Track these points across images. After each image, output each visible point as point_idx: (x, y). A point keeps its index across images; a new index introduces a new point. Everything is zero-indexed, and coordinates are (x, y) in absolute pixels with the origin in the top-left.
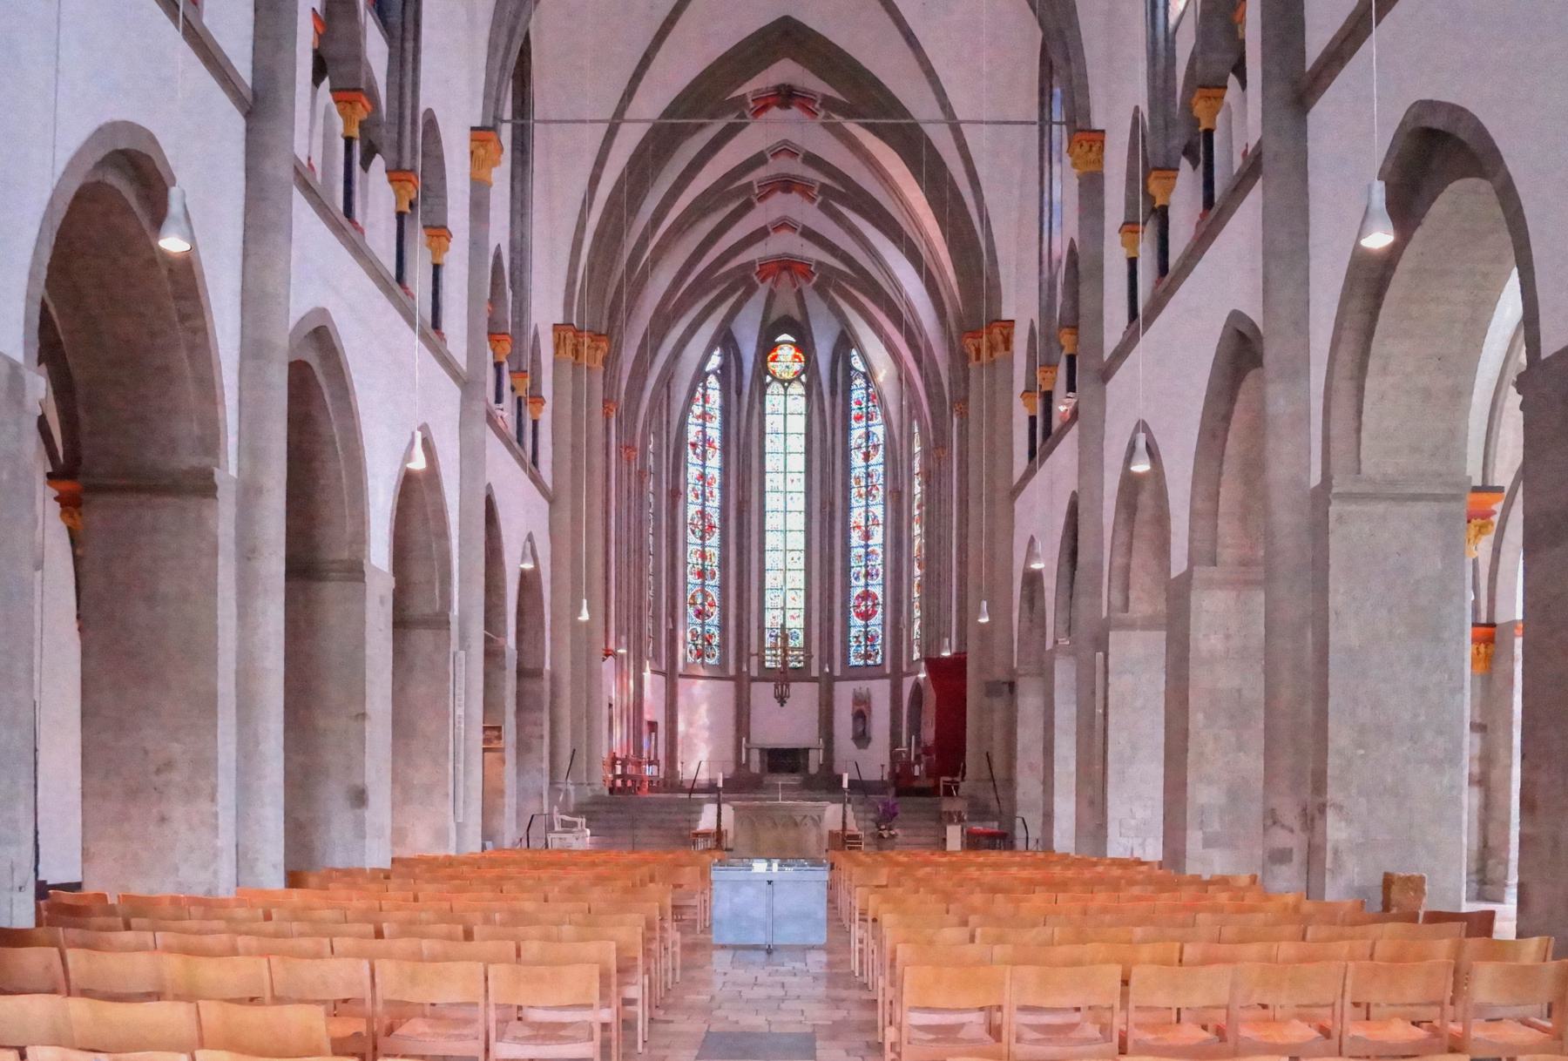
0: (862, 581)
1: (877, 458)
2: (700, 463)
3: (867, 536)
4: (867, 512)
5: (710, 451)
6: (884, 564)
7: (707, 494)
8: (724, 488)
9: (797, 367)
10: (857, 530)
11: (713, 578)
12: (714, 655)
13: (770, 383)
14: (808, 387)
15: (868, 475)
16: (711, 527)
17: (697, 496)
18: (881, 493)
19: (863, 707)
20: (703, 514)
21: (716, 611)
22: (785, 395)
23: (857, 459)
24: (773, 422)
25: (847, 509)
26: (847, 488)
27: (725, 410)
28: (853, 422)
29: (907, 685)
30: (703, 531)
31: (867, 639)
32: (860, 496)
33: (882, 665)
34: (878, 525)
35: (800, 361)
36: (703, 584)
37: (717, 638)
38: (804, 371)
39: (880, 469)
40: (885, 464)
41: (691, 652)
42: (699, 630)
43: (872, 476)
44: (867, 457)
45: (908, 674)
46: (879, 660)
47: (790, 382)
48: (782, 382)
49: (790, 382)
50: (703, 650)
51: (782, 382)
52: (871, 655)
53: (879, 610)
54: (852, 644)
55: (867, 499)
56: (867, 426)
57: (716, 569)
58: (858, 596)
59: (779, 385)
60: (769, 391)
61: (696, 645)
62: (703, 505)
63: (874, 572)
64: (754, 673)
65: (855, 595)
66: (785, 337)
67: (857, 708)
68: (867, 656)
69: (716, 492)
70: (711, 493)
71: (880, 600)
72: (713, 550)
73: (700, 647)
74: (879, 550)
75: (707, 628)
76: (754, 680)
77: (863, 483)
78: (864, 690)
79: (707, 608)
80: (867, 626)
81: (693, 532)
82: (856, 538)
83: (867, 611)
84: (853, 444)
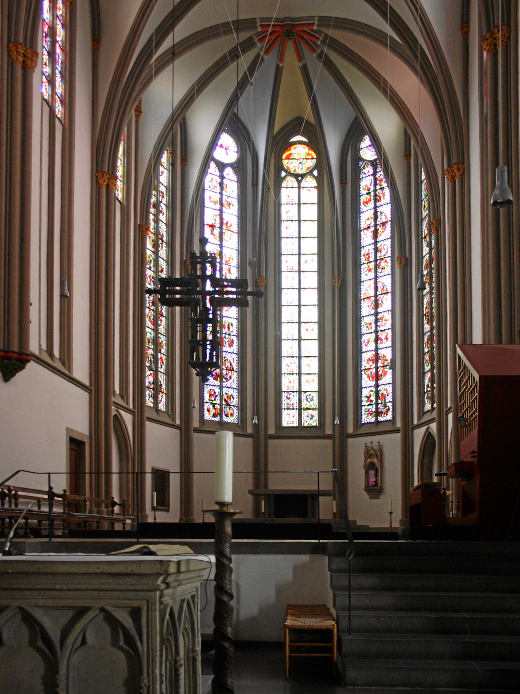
0: (372, 346)
1: (386, 234)
2: (219, 243)
4: (376, 283)
9: (311, 163)
10: (366, 301)
11: (231, 345)
12: (232, 415)
13: (285, 177)
14: (319, 179)
15: (376, 250)
18: (389, 264)
19: (375, 460)
22: (299, 188)
23: (366, 238)
25: (357, 282)
26: (357, 265)
28: (362, 206)
29: (419, 435)
33: (393, 421)
34: (387, 293)
35: (313, 158)
37: (236, 399)
38: (316, 167)
39: (388, 243)
40: (392, 238)
41: (208, 410)
42: (217, 391)
43: (381, 251)
44: (376, 234)
45: (419, 426)
46: (389, 417)
47: (303, 176)
48: (296, 176)
49: (303, 176)
50: (221, 409)
51: (296, 176)
52: (381, 412)
55: (376, 271)
56: (375, 207)
57: (235, 339)
58: (369, 360)
59: (294, 179)
60: (284, 184)
61: (214, 405)
64: (271, 431)
65: (366, 360)
66: (299, 138)
67: (369, 460)
68: (378, 413)
70: (229, 271)
73: (218, 406)
74: (388, 316)
75: (224, 390)
76: (272, 437)
77: (372, 259)
78: (375, 446)
80: (377, 386)
82: (366, 308)
83: (377, 372)
84: (363, 225)
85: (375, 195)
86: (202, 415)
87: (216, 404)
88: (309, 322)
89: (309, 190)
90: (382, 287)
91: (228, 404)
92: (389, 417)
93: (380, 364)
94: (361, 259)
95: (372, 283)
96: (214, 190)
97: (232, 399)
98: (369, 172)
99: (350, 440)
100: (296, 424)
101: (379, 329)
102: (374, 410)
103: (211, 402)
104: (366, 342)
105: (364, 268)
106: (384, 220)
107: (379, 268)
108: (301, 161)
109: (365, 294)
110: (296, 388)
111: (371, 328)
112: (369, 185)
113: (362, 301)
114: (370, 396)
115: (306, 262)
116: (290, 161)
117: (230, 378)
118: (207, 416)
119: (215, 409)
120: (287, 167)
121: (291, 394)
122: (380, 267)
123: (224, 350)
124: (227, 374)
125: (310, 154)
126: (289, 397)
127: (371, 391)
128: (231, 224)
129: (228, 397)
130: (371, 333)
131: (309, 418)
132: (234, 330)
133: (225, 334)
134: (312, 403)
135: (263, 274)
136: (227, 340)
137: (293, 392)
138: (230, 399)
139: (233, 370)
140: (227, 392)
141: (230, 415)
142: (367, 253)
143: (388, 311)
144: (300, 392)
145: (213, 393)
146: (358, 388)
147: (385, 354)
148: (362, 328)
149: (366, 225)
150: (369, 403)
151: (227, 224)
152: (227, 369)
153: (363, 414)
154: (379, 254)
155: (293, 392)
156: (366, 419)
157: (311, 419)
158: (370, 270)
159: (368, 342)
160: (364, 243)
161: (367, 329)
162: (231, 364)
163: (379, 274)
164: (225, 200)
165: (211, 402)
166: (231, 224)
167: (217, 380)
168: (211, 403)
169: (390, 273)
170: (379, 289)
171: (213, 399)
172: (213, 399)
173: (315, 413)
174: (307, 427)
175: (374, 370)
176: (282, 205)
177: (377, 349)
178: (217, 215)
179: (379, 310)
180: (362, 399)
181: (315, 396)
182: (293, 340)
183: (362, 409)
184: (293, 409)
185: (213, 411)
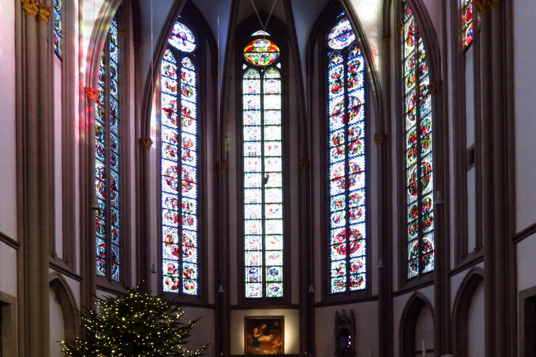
0: (343, 222)
2: (176, 127)
3: (347, 183)
5: (185, 121)
6: (367, 204)
8: (201, 151)
12: (192, 287)
15: (347, 133)
16: (189, 182)
17: (172, 154)
18: (363, 145)
19: (347, 326)
22: (262, 79)
26: (325, 149)
27: (201, 86)
30: (179, 183)
32: (339, 152)
34: (360, 172)
35: (276, 52)
37: (196, 273)
46: (363, 286)
47: (267, 68)
49: (267, 68)
54: (333, 275)
57: (194, 218)
58: (339, 235)
59: (255, 71)
60: (245, 76)
61: (173, 279)
63: (356, 212)
65: (335, 235)
67: (340, 327)
69: (193, 154)
72: (190, 201)
73: (177, 280)
75: (184, 265)
77: (342, 142)
78: (348, 314)
80: (348, 259)
82: (335, 188)
85: (346, 81)
86: (161, 286)
87: (175, 277)
88: (274, 203)
89: (273, 82)
90: (354, 167)
91: (188, 278)
92: (363, 286)
93: (352, 239)
94: (329, 143)
95: (342, 165)
96: (172, 77)
97: (192, 273)
98: (338, 60)
99: (318, 310)
100: (260, 296)
101: (350, 206)
102: (345, 281)
103: (170, 275)
105: (333, 151)
106: (356, 103)
107: (351, 150)
108: (264, 54)
109: (335, 175)
110: (260, 263)
111: (341, 206)
112: (338, 73)
113: (331, 182)
114: (340, 269)
115: (270, 148)
116: (251, 54)
118: (166, 288)
119: (175, 282)
120: (248, 59)
121: (254, 269)
122: (352, 148)
123: (183, 228)
124: (186, 250)
125: (274, 48)
126: (252, 271)
127: (342, 264)
128: (189, 110)
129: (187, 271)
130: (342, 210)
131: (273, 290)
132: (194, 209)
133: (185, 213)
134: (276, 277)
136: (186, 218)
137: (257, 267)
138: (190, 273)
139: (193, 246)
140: (186, 267)
141: (190, 288)
142: (336, 136)
143: (362, 189)
144: (264, 267)
145: (172, 267)
146: (327, 262)
147: (357, 229)
148: (331, 206)
149: (335, 111)
150: (339, 275)
151: (185, 109)
152: (186, 245)
153: (332, 285)
154: (350, 137)
155: (257, 267)
156: (335, 290)
157: (276, 291)
158: (339, 152)
159: (338, 220)
160: (332, 128)
161: (337, 207)
162: (191, 241)
163: (350, 155)
164: (183, 87)
165: (170, 275)
166: (189, 110)
167: (176, 255)
168: (170, 277)
169: (363, 153)
170: (351, 169)
171: (172, 272)
172: (172, 272)
173: (280, 286)
174: (271, 298)
175: (345, 245)
176: (244, 96)
178: (174, 101)
179: (351, 188)
180: (332, 271)
181: (280, 270)
182: (256, 219)
183: (331, 281)
184: (257, 282)
185: (172, 284)
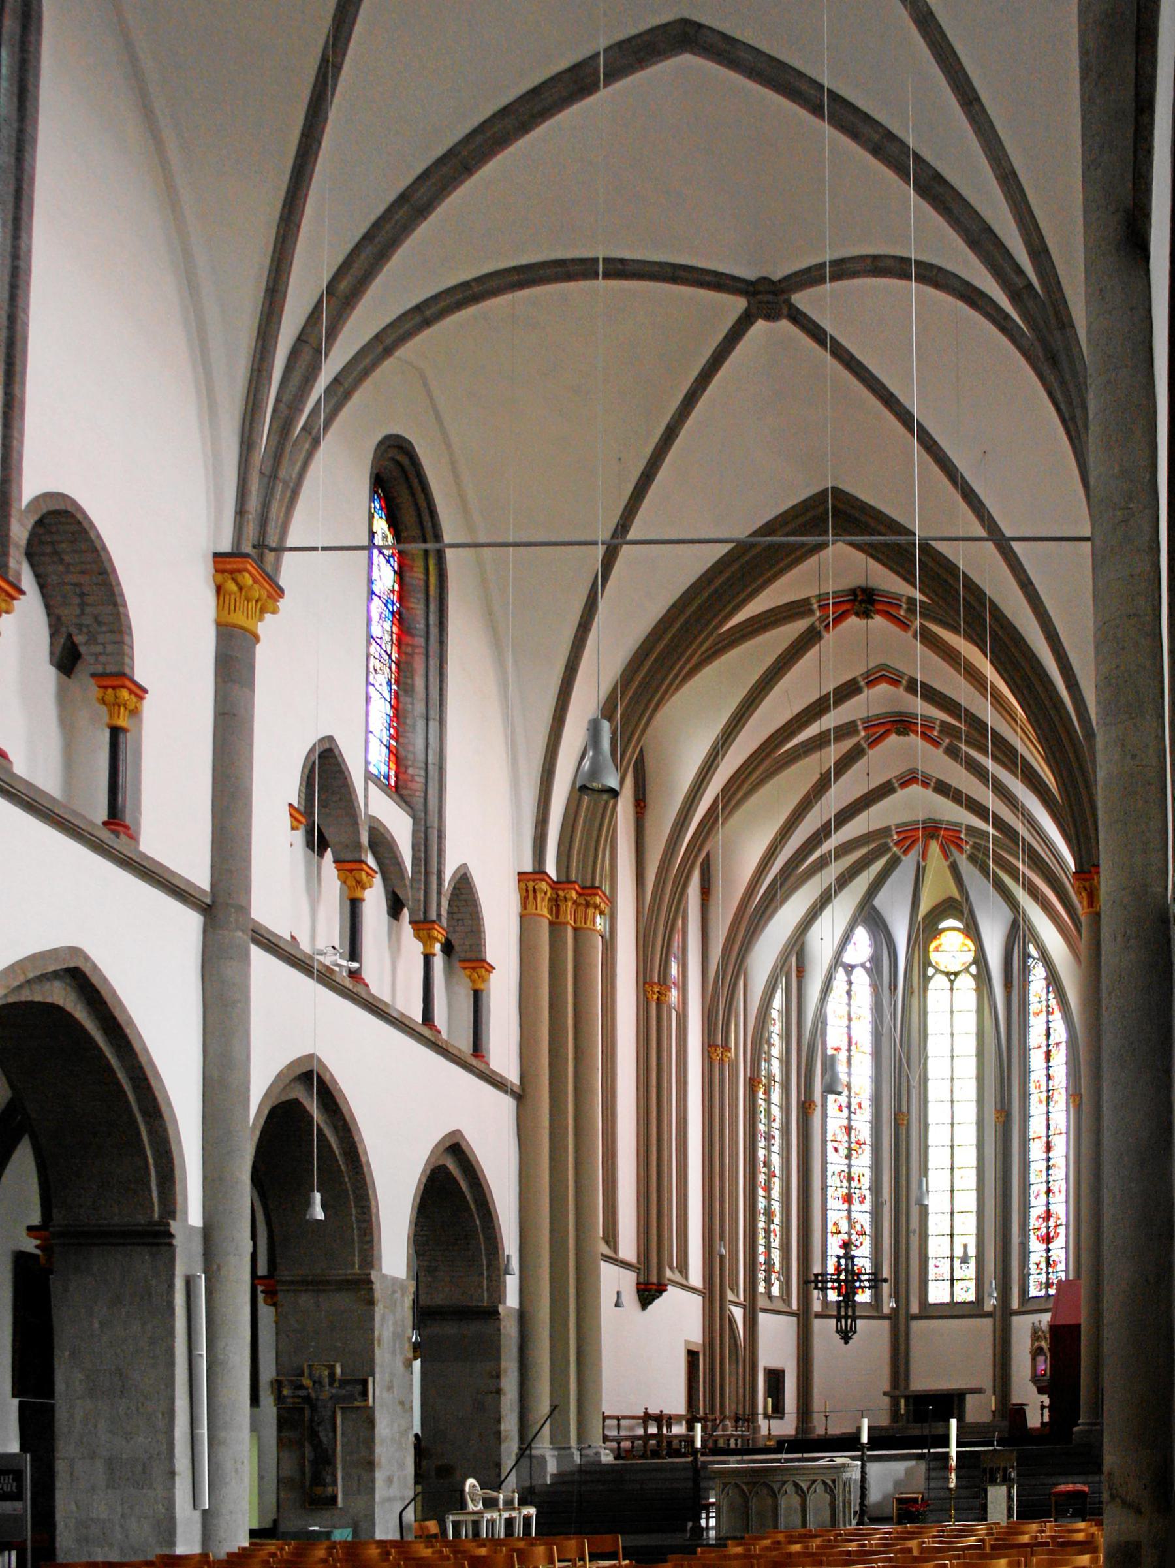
7: (854, 1106)
11: (862, 1201)
13: (933, 976)
14: (977, 978)
20: (848, 1129)
21: (867, 1241)
24: (936, 1023)
25: (1025, 1117)
30: (849, 1149)
31: (1048, 1264)
32: (1041, 1102)
36: (849, 1211)
44: (1048, 1055)
47: (956, 974)
48: (947, 974)
53: (1062, 1230)
54: (1032, 1271)
57: (867, 1193)
58: (1039, 1217)
60: (932, 985)
62: (849, 1119)
67: (1036, 1344)
71: (1063, 1220)
77: (1044, 1088)
79: (854, 1237)
80: (1048, 1250)
81: (836, 1150)
83: (1048, 1233)
93: (1052, 1223)
102: (1044, 1280)
104: (1036, 1194)
113: (1031, 1141)
117: (861, 1244)
135: (904, 1109)
159: (1038, 1195)
177: (1048, 1204)
